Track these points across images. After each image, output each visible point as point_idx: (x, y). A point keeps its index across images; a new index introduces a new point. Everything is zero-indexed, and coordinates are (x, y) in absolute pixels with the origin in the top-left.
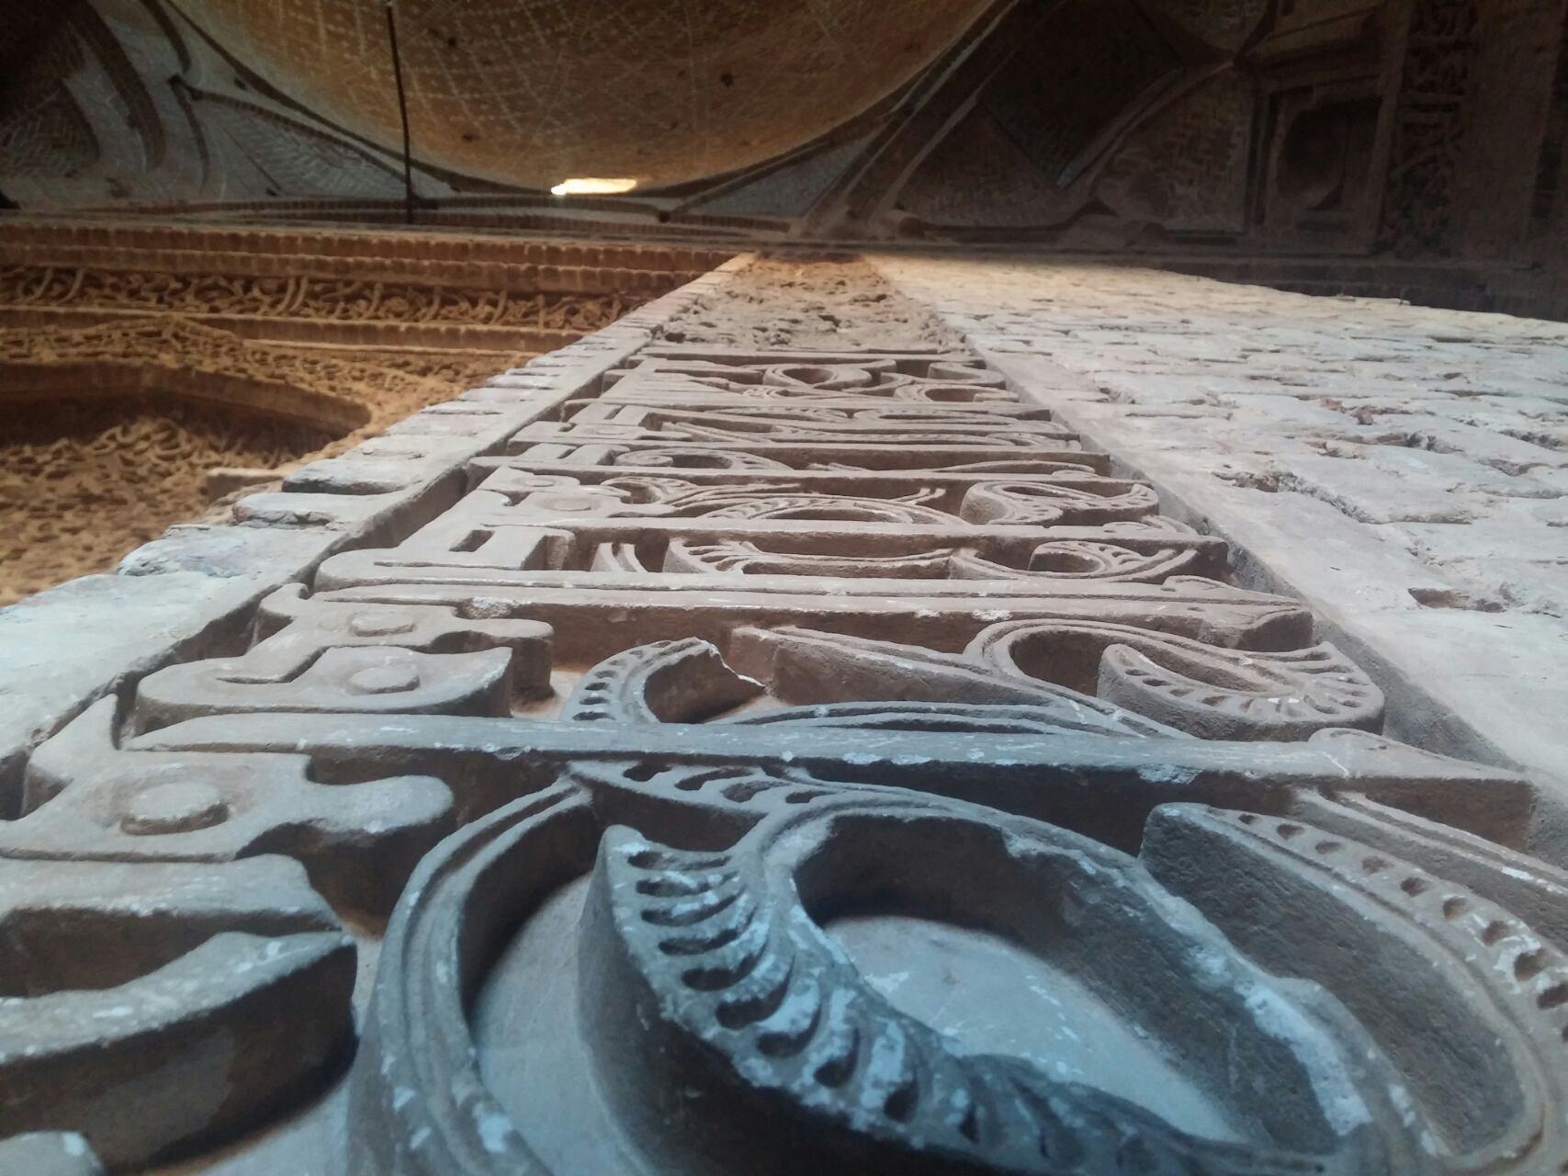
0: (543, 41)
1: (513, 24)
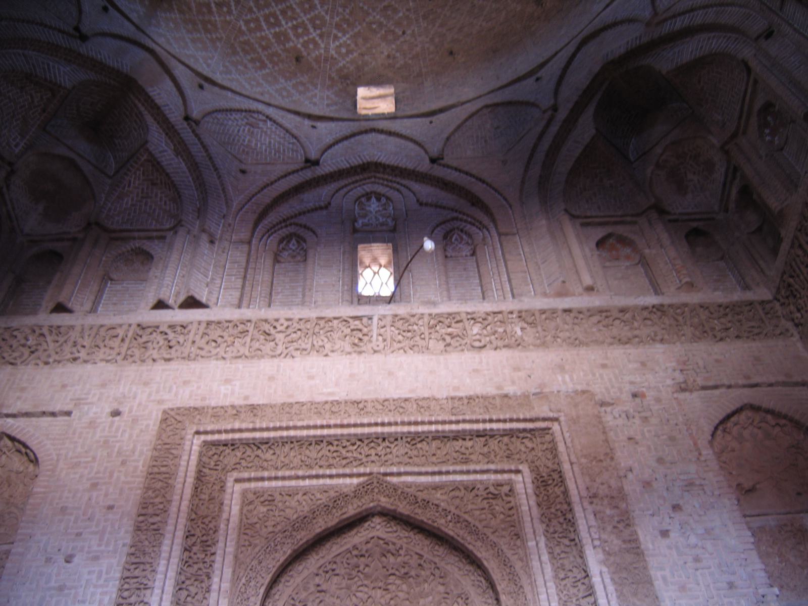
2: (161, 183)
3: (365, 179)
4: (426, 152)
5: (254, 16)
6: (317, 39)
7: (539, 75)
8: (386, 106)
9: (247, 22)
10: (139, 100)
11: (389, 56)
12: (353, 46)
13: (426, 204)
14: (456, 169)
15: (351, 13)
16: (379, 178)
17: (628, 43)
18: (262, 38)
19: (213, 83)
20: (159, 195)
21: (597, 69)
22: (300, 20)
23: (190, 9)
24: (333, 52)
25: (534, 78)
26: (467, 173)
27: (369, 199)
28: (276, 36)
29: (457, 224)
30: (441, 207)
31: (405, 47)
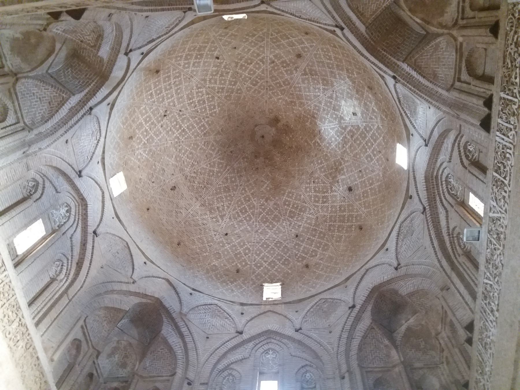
0: (175, 135)
1: (178, 126)
2: (51, 108)
3: (76, 201)
4: (98, 226)
5: (148, 111)
6: (143, 142)
7: (148, 262)
8: (116, 193)
9: (145, 109)
10: (96, 83)
11: (140, 179)
12: (142, 160)
13: (71, 241)
14: (93, 246)
15: (158, 154)
16: (79, 207)
17: (171, 306)
18: (138, 118)
19: (111, 109)
20: (44, 108)
21: (156, 296)
22: (150, 132)
23: (147, 83)
24: (137, 152)
25: (145, 260)
26: (92, 253)
27: (67, 206)
28: (141, 124)
29: (65, 261)
30: (72, 248)
31: (147, 186)
